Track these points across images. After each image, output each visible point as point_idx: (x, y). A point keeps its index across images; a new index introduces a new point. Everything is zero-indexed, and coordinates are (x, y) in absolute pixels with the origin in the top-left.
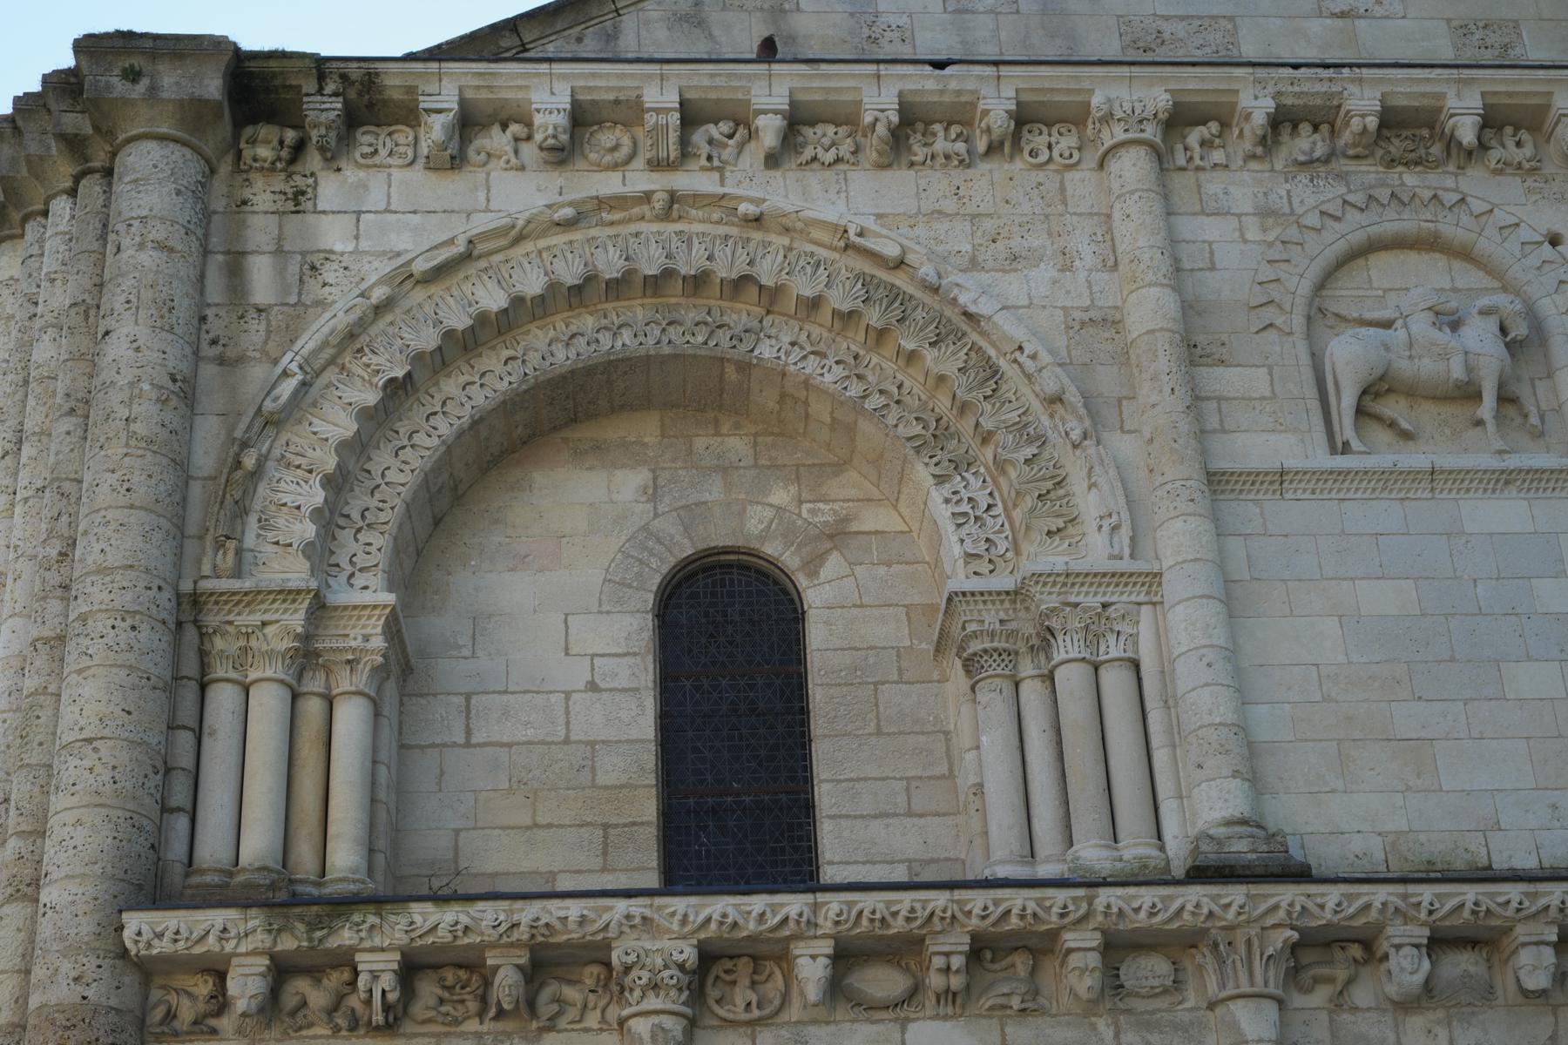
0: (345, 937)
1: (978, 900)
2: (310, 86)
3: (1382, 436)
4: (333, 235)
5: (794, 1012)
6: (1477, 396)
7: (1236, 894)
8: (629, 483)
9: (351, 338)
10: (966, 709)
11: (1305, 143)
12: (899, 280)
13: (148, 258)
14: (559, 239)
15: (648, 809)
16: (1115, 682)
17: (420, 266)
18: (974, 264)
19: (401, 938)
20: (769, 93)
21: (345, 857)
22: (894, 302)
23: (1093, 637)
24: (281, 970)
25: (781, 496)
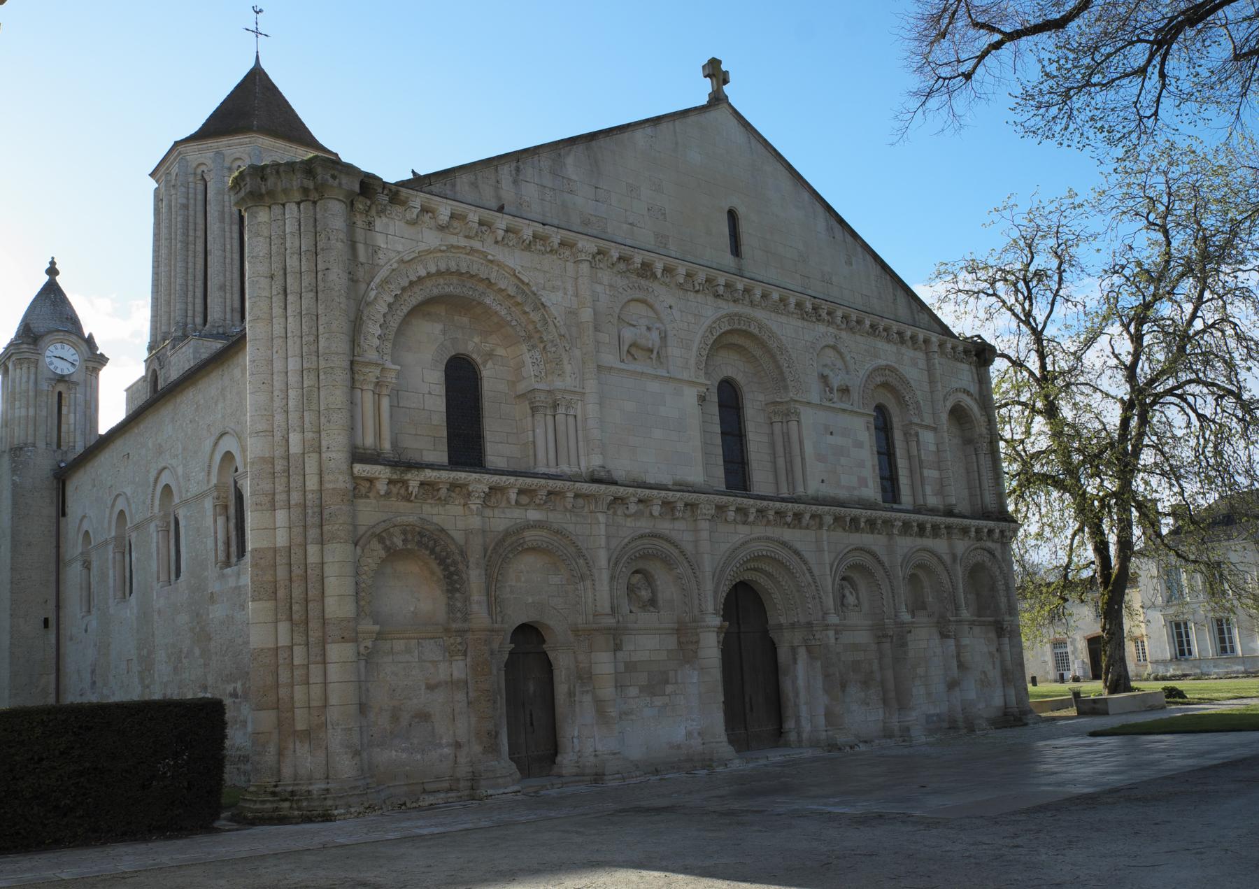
0: (409, 476)
1: (551, 482)
2: (380, 190)
3: (630, 358)
4: (380, 241)
5: (503, 504)
6: (651, 351)
7: (603, 487)
8: (437, 328)
9: (386, 281)
10: (529, 419)
11: (622, 266)
12: (525, 288)
13: (339, 245)
14: (439, 255)
15: (444, 433)
16: (571, 420)
17: (406, 258)
18: (544, 288)
19: (422, 478)
20: (502, 222)
21: (387, 446)
22: (526, 296)
23: (568, 407)
24: (391, 482)
25: (476, 340)
